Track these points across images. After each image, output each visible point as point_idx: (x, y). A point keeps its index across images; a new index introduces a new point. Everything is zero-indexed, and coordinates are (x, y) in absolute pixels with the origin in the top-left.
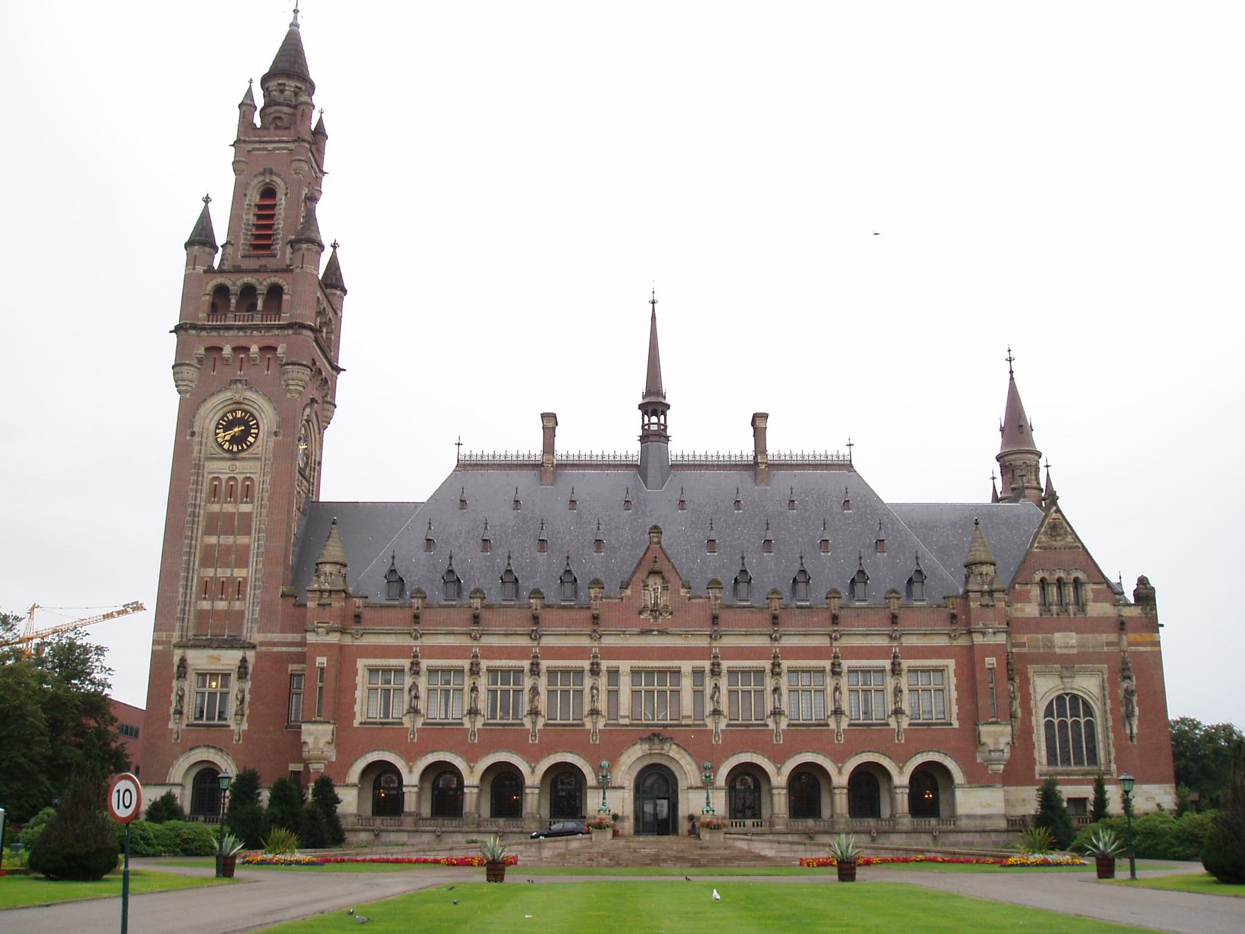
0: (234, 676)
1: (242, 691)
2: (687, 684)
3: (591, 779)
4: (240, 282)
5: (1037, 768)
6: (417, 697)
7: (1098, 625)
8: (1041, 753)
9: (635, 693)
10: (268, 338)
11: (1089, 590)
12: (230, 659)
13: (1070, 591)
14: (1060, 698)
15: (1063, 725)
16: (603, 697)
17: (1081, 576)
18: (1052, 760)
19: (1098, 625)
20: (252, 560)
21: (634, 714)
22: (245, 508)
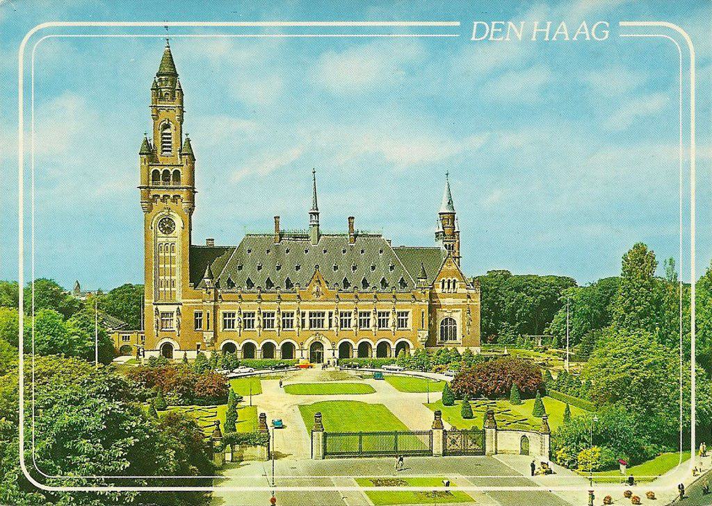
0: (175, 314)
1: (178, 319)
2: (327, 315)
3: (297, 347)
4: (163, 170)
5: (437, 342)
6: (241, 322)
7: (461, 295)
8: (439, 337)
9: (311, 320)
10: (177, 192)
11: (457, 285)
12: (173, 308)
13: (451, 285)
14: (446, 319)
15: (446, 327)
16: (300, 321)
17: (457, 280)
18: (442, 339)
19: (461, 295)
20: (178, 273)
21: (311, 326)
22: (172, 255)
